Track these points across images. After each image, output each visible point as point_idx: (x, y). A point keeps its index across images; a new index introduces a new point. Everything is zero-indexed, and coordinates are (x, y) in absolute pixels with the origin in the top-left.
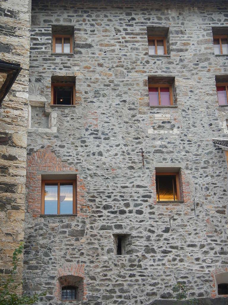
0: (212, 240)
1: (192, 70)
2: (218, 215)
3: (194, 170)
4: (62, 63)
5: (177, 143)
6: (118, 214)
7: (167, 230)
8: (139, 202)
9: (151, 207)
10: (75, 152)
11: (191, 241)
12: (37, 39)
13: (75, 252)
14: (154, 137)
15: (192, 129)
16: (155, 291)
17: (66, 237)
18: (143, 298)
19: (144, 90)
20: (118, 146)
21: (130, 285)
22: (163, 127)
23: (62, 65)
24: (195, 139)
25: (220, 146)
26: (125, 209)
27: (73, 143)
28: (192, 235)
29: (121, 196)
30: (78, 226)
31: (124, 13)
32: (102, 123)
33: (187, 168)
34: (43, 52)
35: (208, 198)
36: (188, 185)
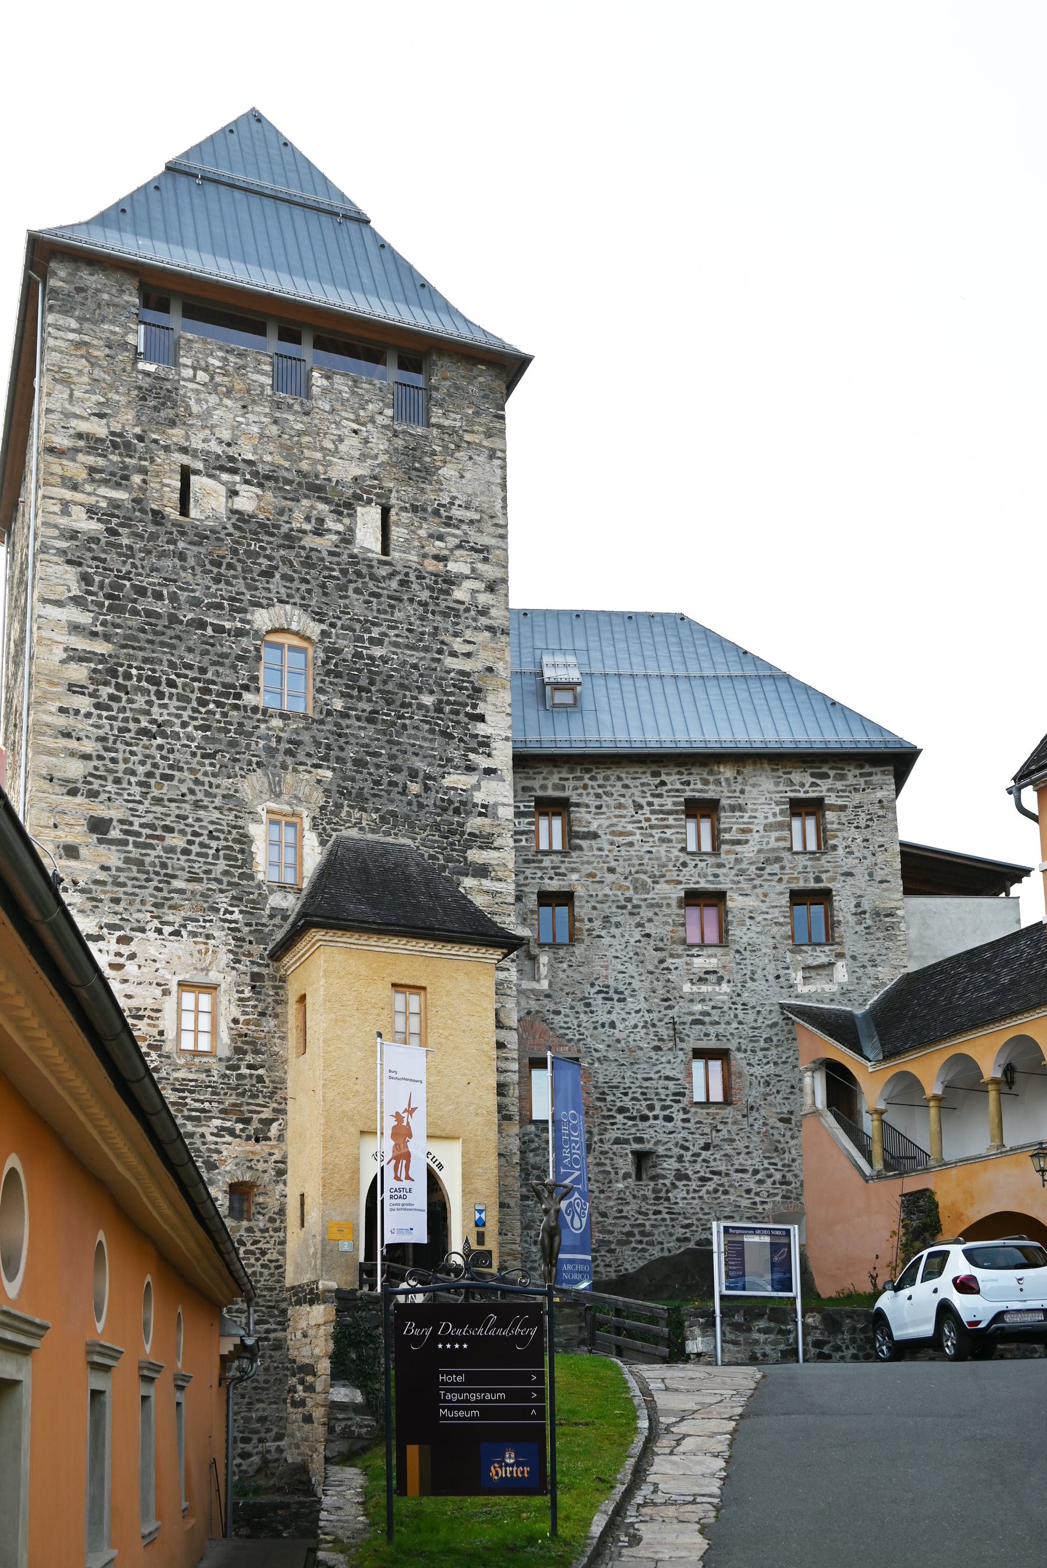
0: (770, 1164)
1: (753, 879)
2: (780, 1125)
3: (749, 1052)
4: (553, 868)
5: (725, 1009)
6: (638, 1122)
7: (706, 1147)
8: (668, 1103)
9: (685, 1111)
10: (575, 1022)
11: (740, 1164)
14: (691, 997)
15: (750, 984)
16: (688, 1235)
18: (671, 1244)
19: (678, 915)
20: (638, 1012)
21: (653, 1226)
22: (706, 980)
23: (552, 871)
24: (752, 1002)
25: (790, 1015)
27: (572, 1008)
28: (742, 1155)
29: (643, 1094)
31: (649, 771)
32: (615, 973)
33: (739, 1050)
34: (523, 847)
35: (769, 1098)
36: (740, 1078)
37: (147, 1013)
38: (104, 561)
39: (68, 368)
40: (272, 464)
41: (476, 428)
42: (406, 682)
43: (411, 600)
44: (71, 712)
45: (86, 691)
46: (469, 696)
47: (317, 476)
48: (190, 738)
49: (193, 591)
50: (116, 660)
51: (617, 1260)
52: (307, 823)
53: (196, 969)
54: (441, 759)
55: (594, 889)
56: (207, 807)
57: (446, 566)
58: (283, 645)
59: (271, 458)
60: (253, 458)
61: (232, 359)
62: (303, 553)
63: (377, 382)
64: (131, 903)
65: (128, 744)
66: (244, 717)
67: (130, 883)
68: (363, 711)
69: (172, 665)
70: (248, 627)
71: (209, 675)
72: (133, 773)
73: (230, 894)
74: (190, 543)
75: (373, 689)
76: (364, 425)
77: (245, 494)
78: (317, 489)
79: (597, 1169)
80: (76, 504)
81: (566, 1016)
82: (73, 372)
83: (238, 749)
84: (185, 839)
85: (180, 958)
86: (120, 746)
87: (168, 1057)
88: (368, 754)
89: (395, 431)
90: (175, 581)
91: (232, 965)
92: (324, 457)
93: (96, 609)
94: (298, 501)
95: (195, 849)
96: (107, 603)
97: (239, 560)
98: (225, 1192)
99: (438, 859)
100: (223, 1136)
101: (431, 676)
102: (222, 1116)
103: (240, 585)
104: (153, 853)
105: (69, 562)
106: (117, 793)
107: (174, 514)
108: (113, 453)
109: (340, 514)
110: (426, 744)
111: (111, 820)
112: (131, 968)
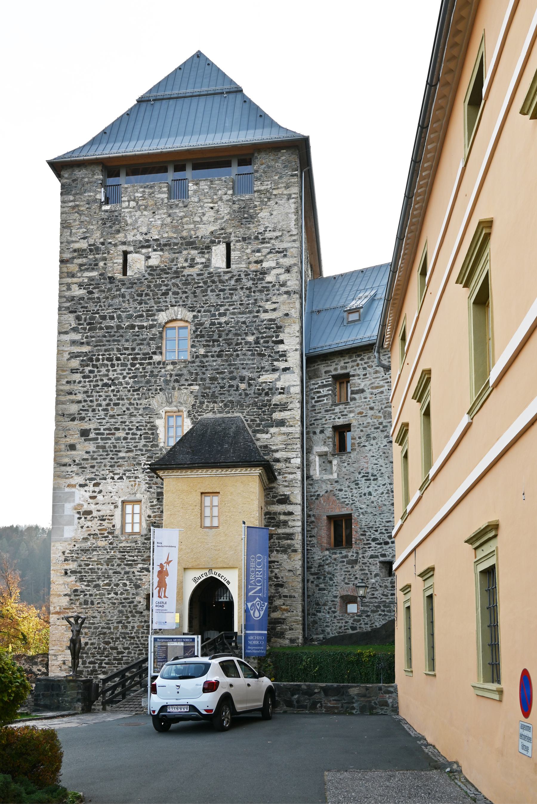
6: (383, 545)
10: (350, 494)
12: (319, 392)
13: (351, 577)
17: (345, 566)
20: (384, 485)
26: (388, 540)
27: (349, 487)
29: (386, 530)
30: (353, 556)
32: (372, 465)
37: (107, 518)
38: (86, 307)
39: (69, 220)
40: (168, 237)
41: (279, 186)
42: (239, 332)
43: (242, 288)
44: (72, 382)
45: (78, 371)
46: (274, 332)
47: (191, 237)
48: (127, 383)
49: (129, 311)
50: (92, 354)
51: (371, 621)
52: (185, 414)
53: (130, 494)
54: (258, 368)
55: (362, 420)
56: (136, 415)
57: (262, 265)
58: (175, 327)
59: (168, 234)
60: (158, 238)
61: (147, 190)
62: (184, 278)
63: (223, 178)
64: (100, 467)
65: (98, 392)
66: (153, 368)
67: (99, 458)
68: (215, 352)
69: (118, 350)
70: (155, 323)
71: (136, 351)
72: (100, 405)
73: (146, 456)
74: (127, 288)
75: (220, 339)
76: (215, 203)
77: (154, 256)
78: (191, 244)
79: (360, 572)
80: (73, 283)
81: (345, 491)
82: (71, 221)
83: (150, 384)
84: (125, 432)
85: (122, 489)
86: (94, 394)
87: (117, 537)
88: (218, 373)
89: (234, 201)
90: (120, 309)
91: (148, 489)
92: (195, 226)
93: (83, 331)
94: (181, 252)
95: (130, 436)
96: (88, 327)
97: (151, 291)
98: (144, 598)
99: (256, 421)
100: (143, 572)
101: (252, 326)
102: (143, 562)
103: (152, 303)
104: (110, 442)
105: (71, 312)
106: (93, 416)
107: (119, 276)
108: (90, 254)
109: (203, 253)
110: (249, 362)
111: (90, 429)
112: (100, 497)
